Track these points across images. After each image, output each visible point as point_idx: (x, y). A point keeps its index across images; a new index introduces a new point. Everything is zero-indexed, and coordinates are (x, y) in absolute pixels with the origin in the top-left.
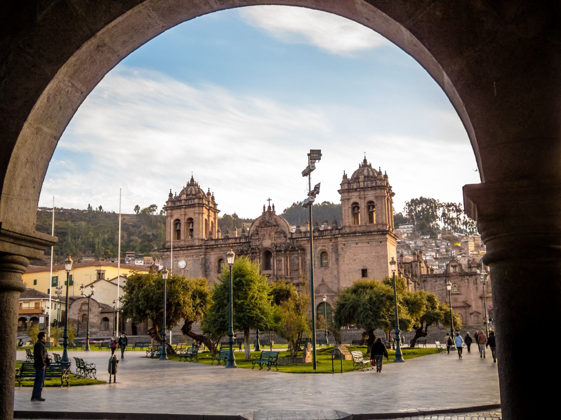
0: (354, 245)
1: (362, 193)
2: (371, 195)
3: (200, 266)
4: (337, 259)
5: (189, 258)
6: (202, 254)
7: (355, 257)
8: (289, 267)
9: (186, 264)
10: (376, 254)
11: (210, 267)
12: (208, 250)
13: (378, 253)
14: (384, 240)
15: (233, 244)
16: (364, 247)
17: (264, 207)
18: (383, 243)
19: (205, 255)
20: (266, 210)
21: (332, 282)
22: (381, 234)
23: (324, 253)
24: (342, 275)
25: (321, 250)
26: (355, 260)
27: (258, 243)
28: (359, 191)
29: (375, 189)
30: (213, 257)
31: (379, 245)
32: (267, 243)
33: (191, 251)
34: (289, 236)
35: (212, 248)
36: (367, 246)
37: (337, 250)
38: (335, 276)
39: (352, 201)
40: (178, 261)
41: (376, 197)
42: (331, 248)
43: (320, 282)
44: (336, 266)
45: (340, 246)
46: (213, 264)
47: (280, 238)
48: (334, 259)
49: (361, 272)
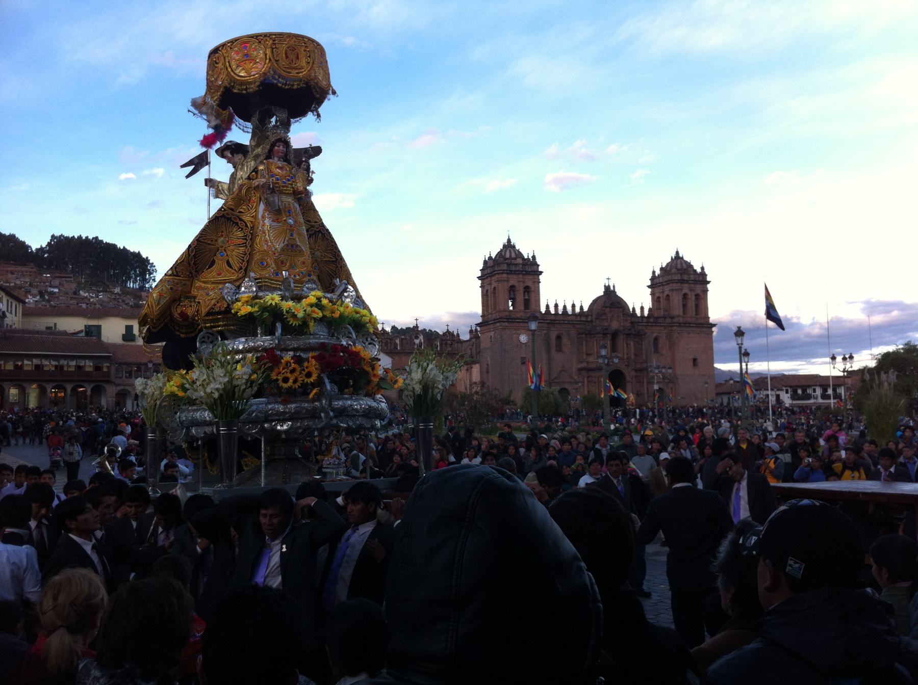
4: (672, 347)
27: (606, 324)
30: (553, 335)
32: (615, 325)
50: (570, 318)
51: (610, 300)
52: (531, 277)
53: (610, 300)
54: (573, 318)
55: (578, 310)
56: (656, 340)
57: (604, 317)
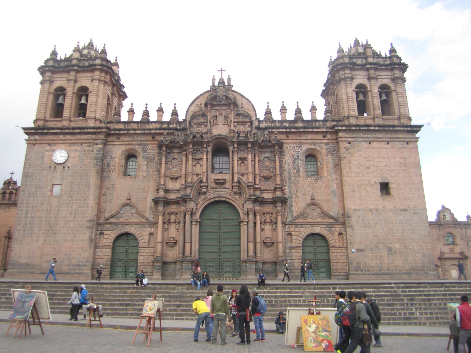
0: (365, 145)
1: (372, 72)
2: (385, 78)
3: (94, 162)
4: (338, 166)
5: (75, 148)
6: (98, 141)
7: (368, 163)
8: (257, 172)
9: (68, 156)
10: (402, 161)
11: (112, 164)
12: (111, 139)
13: (405, 158)
14: (413, 140)
15: (156, 129)
16: (382, 148)
17: (214, 79)
18: (411, 145)
19: (105, 144)
20: (216, 84)
21: (329, 201)
23: (311, 156)
24: (347, 190)
25: (308, 150)
26: (368, 168)
27: (203, 129)
28: (368, 69)
29: (392, 70)
30: (117, 151)
31: (405, 148)
32: (220, 130)
33: (79, 137)
34: (256, 124)
35: (118, 134)
37: (338, 150)
38: (333, 191)
39: (357, 82)
40: (53, 151)
41: (394, 80)
42: (324, 147)
43: (309, 201)
44: (334, 176)
45: (343, 145)
46: (117, 160)
47: (243, 124)
48: (331, 165)
49: (379, 187)
50: (151, 126)
51: (221, 98)
52: (89, 75)
53: (221, 98)
54: (158, 126)
55: (167, 117)
56: (311, 156)
57: (202, 120)
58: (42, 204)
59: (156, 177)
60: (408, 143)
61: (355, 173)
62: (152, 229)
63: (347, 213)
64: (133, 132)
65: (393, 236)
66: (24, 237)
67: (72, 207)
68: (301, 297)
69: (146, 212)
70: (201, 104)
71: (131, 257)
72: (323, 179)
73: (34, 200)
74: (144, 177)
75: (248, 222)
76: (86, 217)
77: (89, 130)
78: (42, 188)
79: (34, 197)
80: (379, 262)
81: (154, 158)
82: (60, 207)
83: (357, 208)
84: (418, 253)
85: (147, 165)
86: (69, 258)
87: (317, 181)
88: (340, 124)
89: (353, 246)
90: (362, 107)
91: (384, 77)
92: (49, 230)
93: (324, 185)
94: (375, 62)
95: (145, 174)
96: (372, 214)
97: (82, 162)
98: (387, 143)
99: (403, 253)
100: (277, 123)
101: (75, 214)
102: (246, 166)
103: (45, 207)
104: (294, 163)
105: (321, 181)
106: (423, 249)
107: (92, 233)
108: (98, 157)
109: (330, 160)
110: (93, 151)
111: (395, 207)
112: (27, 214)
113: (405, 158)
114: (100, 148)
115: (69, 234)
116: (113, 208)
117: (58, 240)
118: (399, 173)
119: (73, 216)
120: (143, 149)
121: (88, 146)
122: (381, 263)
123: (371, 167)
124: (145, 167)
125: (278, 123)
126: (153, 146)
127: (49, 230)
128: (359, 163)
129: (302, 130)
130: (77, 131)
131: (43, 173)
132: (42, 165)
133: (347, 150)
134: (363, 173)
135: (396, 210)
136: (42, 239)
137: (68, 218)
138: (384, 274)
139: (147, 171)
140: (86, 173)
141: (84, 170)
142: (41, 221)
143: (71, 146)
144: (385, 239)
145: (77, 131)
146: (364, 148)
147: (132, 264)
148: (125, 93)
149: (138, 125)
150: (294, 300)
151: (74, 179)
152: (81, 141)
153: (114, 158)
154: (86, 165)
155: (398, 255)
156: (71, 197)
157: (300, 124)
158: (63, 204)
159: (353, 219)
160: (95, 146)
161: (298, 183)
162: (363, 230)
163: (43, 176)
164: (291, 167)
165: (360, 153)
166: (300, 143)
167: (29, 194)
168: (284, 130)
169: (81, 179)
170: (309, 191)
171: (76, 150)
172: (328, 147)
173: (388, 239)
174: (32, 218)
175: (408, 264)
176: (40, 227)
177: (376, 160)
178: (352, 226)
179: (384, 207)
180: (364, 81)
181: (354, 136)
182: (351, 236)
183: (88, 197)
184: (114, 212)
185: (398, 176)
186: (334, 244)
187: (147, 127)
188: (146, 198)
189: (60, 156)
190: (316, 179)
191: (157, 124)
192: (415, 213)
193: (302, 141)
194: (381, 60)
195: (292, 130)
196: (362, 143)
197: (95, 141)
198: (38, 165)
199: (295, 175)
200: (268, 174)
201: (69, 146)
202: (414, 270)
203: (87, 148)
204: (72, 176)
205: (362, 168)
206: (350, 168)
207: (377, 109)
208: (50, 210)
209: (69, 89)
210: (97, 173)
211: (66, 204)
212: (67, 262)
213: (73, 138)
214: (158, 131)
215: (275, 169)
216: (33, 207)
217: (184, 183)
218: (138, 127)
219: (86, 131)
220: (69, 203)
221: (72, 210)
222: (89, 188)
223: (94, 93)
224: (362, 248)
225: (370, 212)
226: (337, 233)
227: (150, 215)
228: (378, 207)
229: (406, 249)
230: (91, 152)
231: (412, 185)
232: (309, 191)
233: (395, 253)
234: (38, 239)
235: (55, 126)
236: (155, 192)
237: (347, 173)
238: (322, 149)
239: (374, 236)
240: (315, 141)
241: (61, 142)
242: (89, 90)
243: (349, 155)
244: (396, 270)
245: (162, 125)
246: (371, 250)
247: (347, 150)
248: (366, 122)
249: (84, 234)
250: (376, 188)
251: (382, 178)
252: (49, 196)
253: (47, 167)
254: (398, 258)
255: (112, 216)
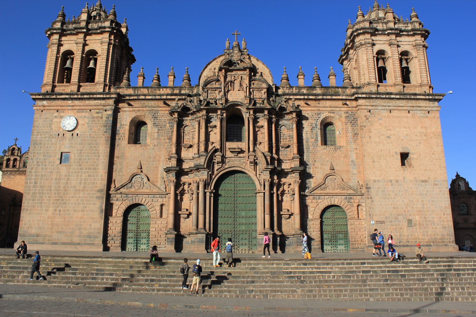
0: (385, 113)
1: (393, 37)
5: (84, 114)
6: (108, 108)
7: (388, 131)
10: (424, 130)
13: (426, 128)
15: (167, 95)
21: (348, 171)
22: (430, 100)
26: (389, 137)
31: (427, 117)
33: (87, 102)
36: (407, 117)
38: (353, 161)
40: (62, 117)
43: (328, 171)
44: (353, 146)
45: (362, 114)
49: (399, 157)
54: (169, 91)
58: (51, 172)
59: (168, 146)
60: (429, 112)
61: (376, 142)
62: (164, 199)
63: (367, 185)
64: (143, 97)
65: (413, 208)
66: (34, 207)
67: (81, 176)
68: (330, 272)
69: (157, 182)
70: (215, 69)
71: (142, 228)
72: (341, 149)
73: (43, 169)
74: (155, 146)
75: (264, 193)
76: (96, 187)
77: (98, 96)
78: (51, 156)
79: (42, 165)
80: (398, 234)
81: (166, 125)
82: (69, 175)
83: (377, 178)
84: (438, 225)
85: (158, 132)
86: (80, 229)
87: (336, 151)
88: (360, 91)
89: (372, 218)
90: (382, 74)
91: (405, 43)
92: (58, 200)
93: (343, 155)
94: (396, 27)
95: (156, 142)
96: (392, 185)
97: (91, 129)
98: (407, 111)
99: (423, 225)
100: (294, 89)
101: (85, 183)
102: (263, 135)
103: (54, 177)
104: (312, 132)
105: (340, 151)
106: (443, 221)
107: (102, 203)
108: (108, 124)
109: (350, 128)
110: (102, 118)
111: (415, 178)
112: (36, 183)
113: (426, 128)
114: (109, 115)
115: (79, 204)
116: (123, 177)
117: (68, 210)
118: (420, 143)
119: (82, 185)
120: (153, 116)
121: (98, 113)
122: (400, 235)
123: (391, 137)
124: (156, 134)
125: (296, 89)
126: (164, 112)
127: (58, 200)
128: (379, 132)
129: (320, 97)
130: (85, 96)
131: (51, 140)
132: (50, 132)
133: (367, 119)
134: (383, 142)
135: (416, 181)
136: (51, 209)
137: (78, 188)
138: (404, 246)
139: (157, 139)
140: (95, 141)
141: (93, 138)
142: (51, 190)
143: (80, 112)
144: (405, 211)
145: (85, 96)
146: (385, 117)
147: (144, 235)
148: (133, 56)
149: (148, 90)
150: (323, 276)
151: (83, 147)
152: (90, 108)
153: (123, 125)
154: (95, 132)
155: (418, 226)
156: (80, 165)
157: (318, 91)
158: (72, 173)
159: (372, 190)
160: (105, 113)
161: (316, 153)
162: (383, 202)
163: (52, 144)
164: (309, 136)
165: (380, 121)
166: (319, 110)
167: (37, 162)
168: (302, 97)
169: (91, 147)
170: (328, 161)
171: (85, 117)
172: (347, 115)
173: (408, 211)
174: (41, 187)
175: (427, 236)
176: (50, 197)
177: (397, 129)
178: (371, 198)
179: (404, 178)
180: (386, 48)
181: (374, 104)
182: (370, 208)
183: (97, 165)
184: (124, 182)
185: (419, 146)
186: (353, 216)
187: (158, 92)
188: (157, 167)
189: (69, 122)
190: (335, 149)
191: (168, 89)
192: (436, 185)
193: (321, 109)
194: (402, 25)
195: (311, 97)
196: (382, 111)
197: (105, 108)
198: (47, 132)
199: (313, 144)
200: (285, 143)
201: (77, 112)
202: (433, 243)
203: (96, 115)
204: (81, 144)
205: (383, 137)
206: (370, 137)
207: (398, 76)
208: (60, 179)
209: (78, 52)
210: (106, 141)
211: (75, 172)
212: (77, 233)
213: (81, 104)
214: (169, 97)
215: (293, 138)
216: (42, 175)
217: (196, 152)
218: (148, 92)
219: (95, 96)
220: (78, 172)
221: (81, 180)
222: (99, 156)
223: (104, 56)
224: (381, 220)
225: (390, 183)
226: (355, 205)
227: (161, 185)
228: (398, 178)
229: (426, 221)
230: (99, 119)
231: (433, 156)
232: (328, 161)
233: (415, 225)
234: (48, 209)
235: (63, 92)
236: (167, 161)
237: (367, 142)
238: (341, 117)
239: (394, 208)
240: (334, 109)
241: (70, 108)
242: (97, 54)
243: (369, 124)
244: (416, 242)
245: (174, 90)
246: (391, 222)
247: (367, 119)
248: (386, 90)
249: (94, 204)
250: (397, 159)
251: (402, 148)
252: (58, 165)
253: (55, 135)
254: (418, 230)
255: (123, 186)
